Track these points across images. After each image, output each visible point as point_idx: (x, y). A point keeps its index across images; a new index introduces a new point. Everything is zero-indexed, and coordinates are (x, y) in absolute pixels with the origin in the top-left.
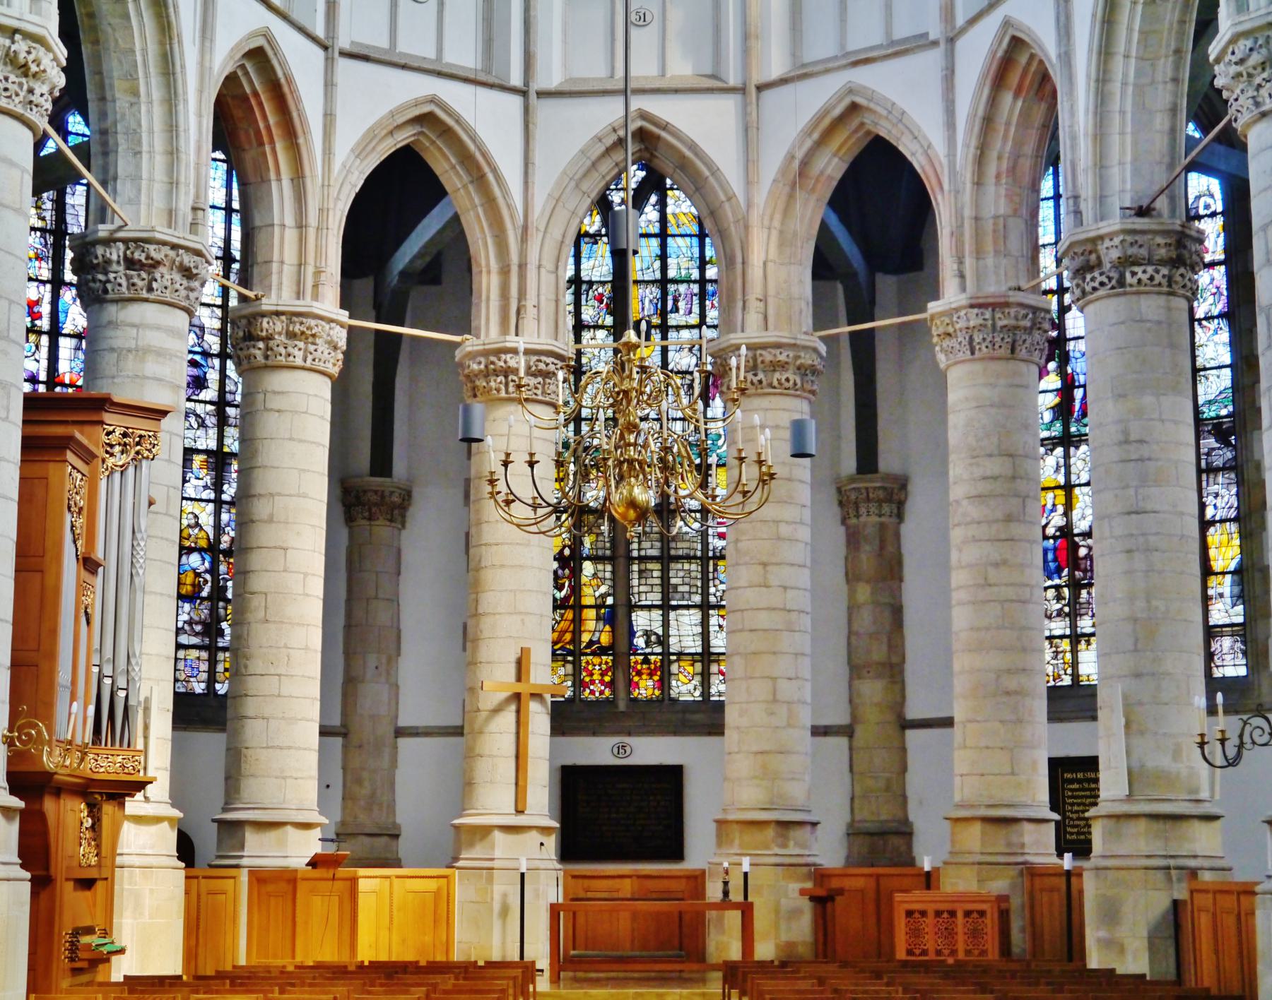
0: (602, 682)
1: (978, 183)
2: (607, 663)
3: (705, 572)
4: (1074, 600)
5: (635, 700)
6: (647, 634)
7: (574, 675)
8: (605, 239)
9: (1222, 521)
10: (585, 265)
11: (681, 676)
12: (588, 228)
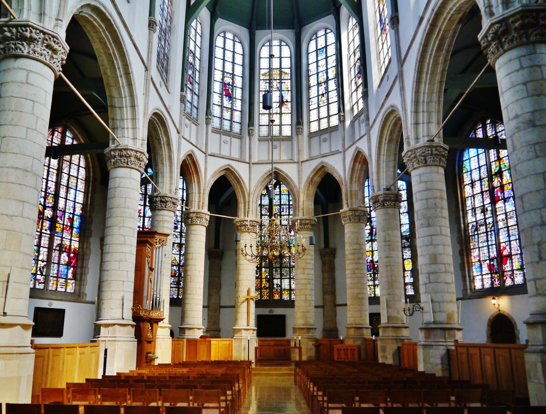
0: (267, 296)
1: (351, 183)
3: (290, 270)
4: (374, 277)
6: (277, 285)
9: (408, 259)
10: (263, 201)
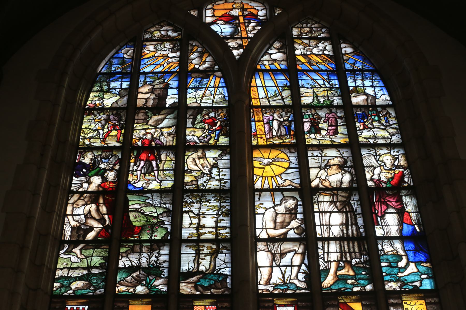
8: (219, 74)
12: (197, 66)
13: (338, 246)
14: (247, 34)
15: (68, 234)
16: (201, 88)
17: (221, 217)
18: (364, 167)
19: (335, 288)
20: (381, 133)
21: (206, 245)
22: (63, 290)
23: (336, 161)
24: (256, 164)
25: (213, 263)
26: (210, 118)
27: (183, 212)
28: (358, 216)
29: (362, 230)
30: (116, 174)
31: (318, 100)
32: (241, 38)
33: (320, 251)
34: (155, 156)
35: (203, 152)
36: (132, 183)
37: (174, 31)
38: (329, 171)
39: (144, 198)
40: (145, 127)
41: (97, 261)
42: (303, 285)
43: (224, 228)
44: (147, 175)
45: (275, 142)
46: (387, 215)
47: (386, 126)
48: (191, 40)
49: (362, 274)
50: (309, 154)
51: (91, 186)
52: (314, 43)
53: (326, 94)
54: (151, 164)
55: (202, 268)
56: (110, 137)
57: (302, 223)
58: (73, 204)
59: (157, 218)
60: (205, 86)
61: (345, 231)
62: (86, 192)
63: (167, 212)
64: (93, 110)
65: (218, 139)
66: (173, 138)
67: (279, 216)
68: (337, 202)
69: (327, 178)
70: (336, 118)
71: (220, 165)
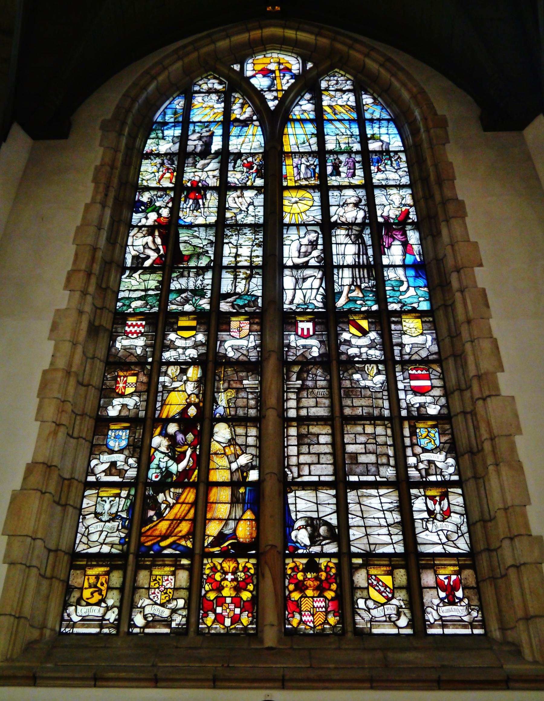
0: (237, 601)
2: (246, 569)
5: (295, 631)
7: (189, 589)
8: (257, 123)
11: (373, 593)
12: (238, 116)
13: (351, 272)
14: (282, 86)
15: (129, 263)
16: (241, 136)
17: (255, 248)
18: (375, 205)
19: (347, 307)
20: (392, 176)
21: (242, 271)
22: (125, 308)
23: (353, 200)
24: (285, 202)
25: (247, 286)
26: (248, 162)
27: (224, 243)
28: (368, 247)
29: (371, 259)
30: (170, 211)
31: (340, 146)
32: (277, 90)
33: (335, 276)
34: (202, 196)
35: (242, 191)
36: (182, 218)
37: (220, 83)
38: (346, 208)
39: (192, 231)
40: (194, 170)
41: (153, 284)
42: (321, 305)
43: (258, 256)
44: (195, 211)
45: (302, 183)
46: (392, 246)
47: (397, 170)
48: (234, 92)
49: (369, 296)
50: (330, 193)
51: (148, 221)
52: (339, 95)
53: (347, 142)
54: (198, 203)
55: (238, 290)
56: (164, 179)
57: (321, 253)
58: (133, 236)
59: (203, 248)
60: (245, 134)
61: (357, 260)
62: (144, 226)
63: (211, 243)
64: (149, 155)
65: (254, 181)
66: (217, 179)
67: (303, 247)
68: (351, 235)
69: (344, 214)
70: (354, 162)
71: (255, 204)
